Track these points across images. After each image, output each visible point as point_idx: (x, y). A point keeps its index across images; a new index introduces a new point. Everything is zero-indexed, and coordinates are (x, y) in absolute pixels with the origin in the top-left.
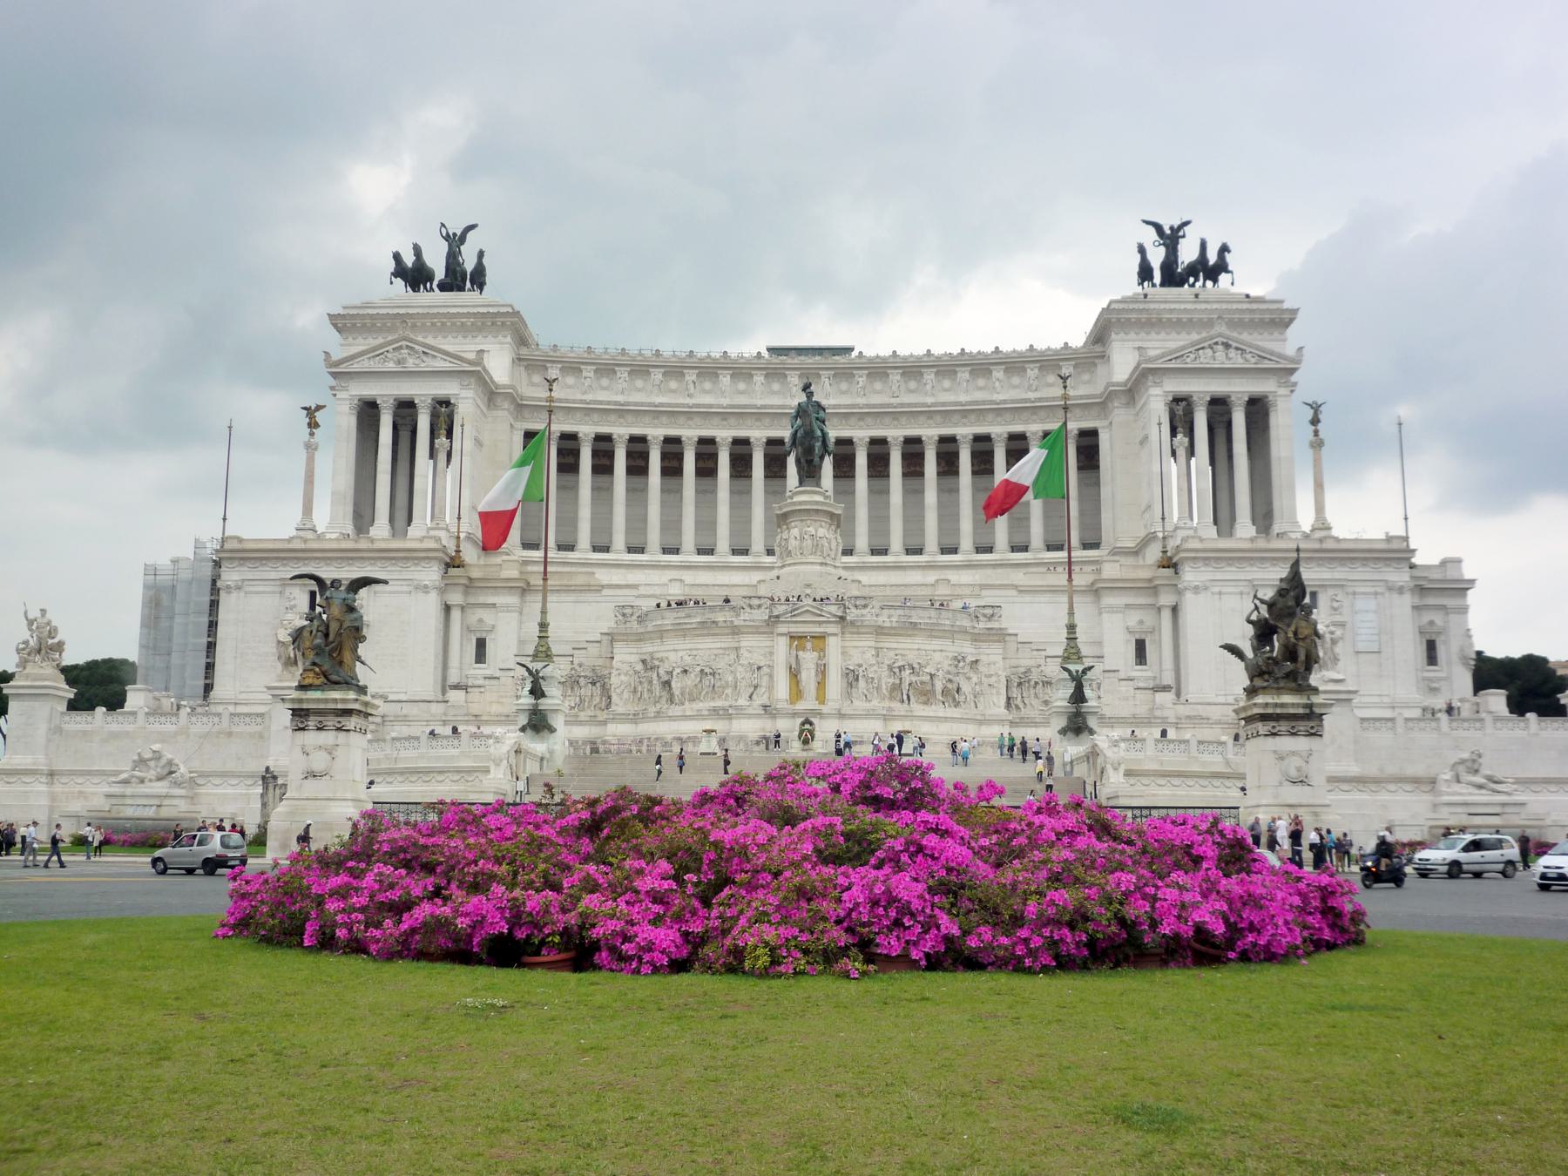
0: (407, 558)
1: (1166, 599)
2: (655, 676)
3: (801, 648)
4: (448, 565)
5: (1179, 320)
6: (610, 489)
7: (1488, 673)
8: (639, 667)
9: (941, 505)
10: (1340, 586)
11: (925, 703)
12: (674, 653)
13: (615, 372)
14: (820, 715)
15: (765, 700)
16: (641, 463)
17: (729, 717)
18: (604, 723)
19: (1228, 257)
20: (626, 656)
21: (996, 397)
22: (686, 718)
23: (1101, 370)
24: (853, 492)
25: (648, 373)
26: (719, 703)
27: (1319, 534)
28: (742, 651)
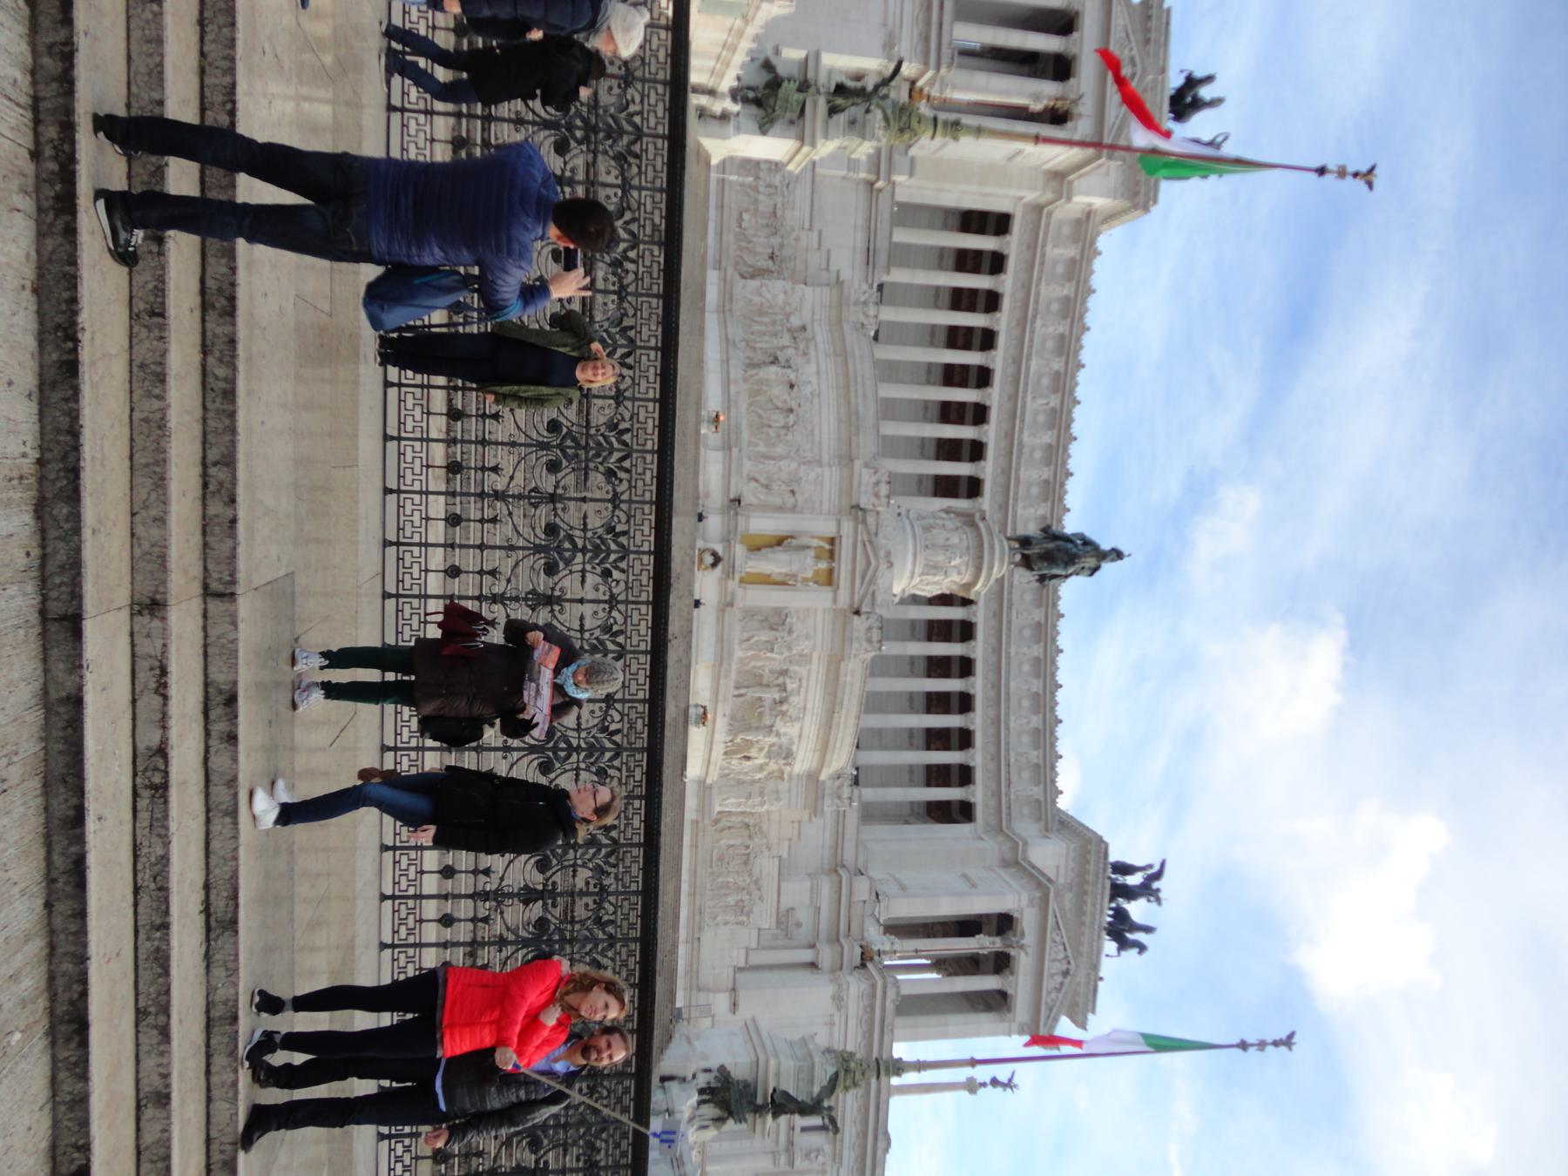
0: (928, 24)
1: (826, 955)
4: (913, 83)
5: (1084, 913)
8: (795, 321)
11: (733, 718)
12: (817, 373)
13: (1065, 317)
15: (748, 498)
16: (961, 341)
17: (727, 447)
18: (718, 265)
19: (1135, 951)
20: (810, 302)
22: (727, 384)
25: (1060, 354)
26: (745, 436)
28: (818, 470)
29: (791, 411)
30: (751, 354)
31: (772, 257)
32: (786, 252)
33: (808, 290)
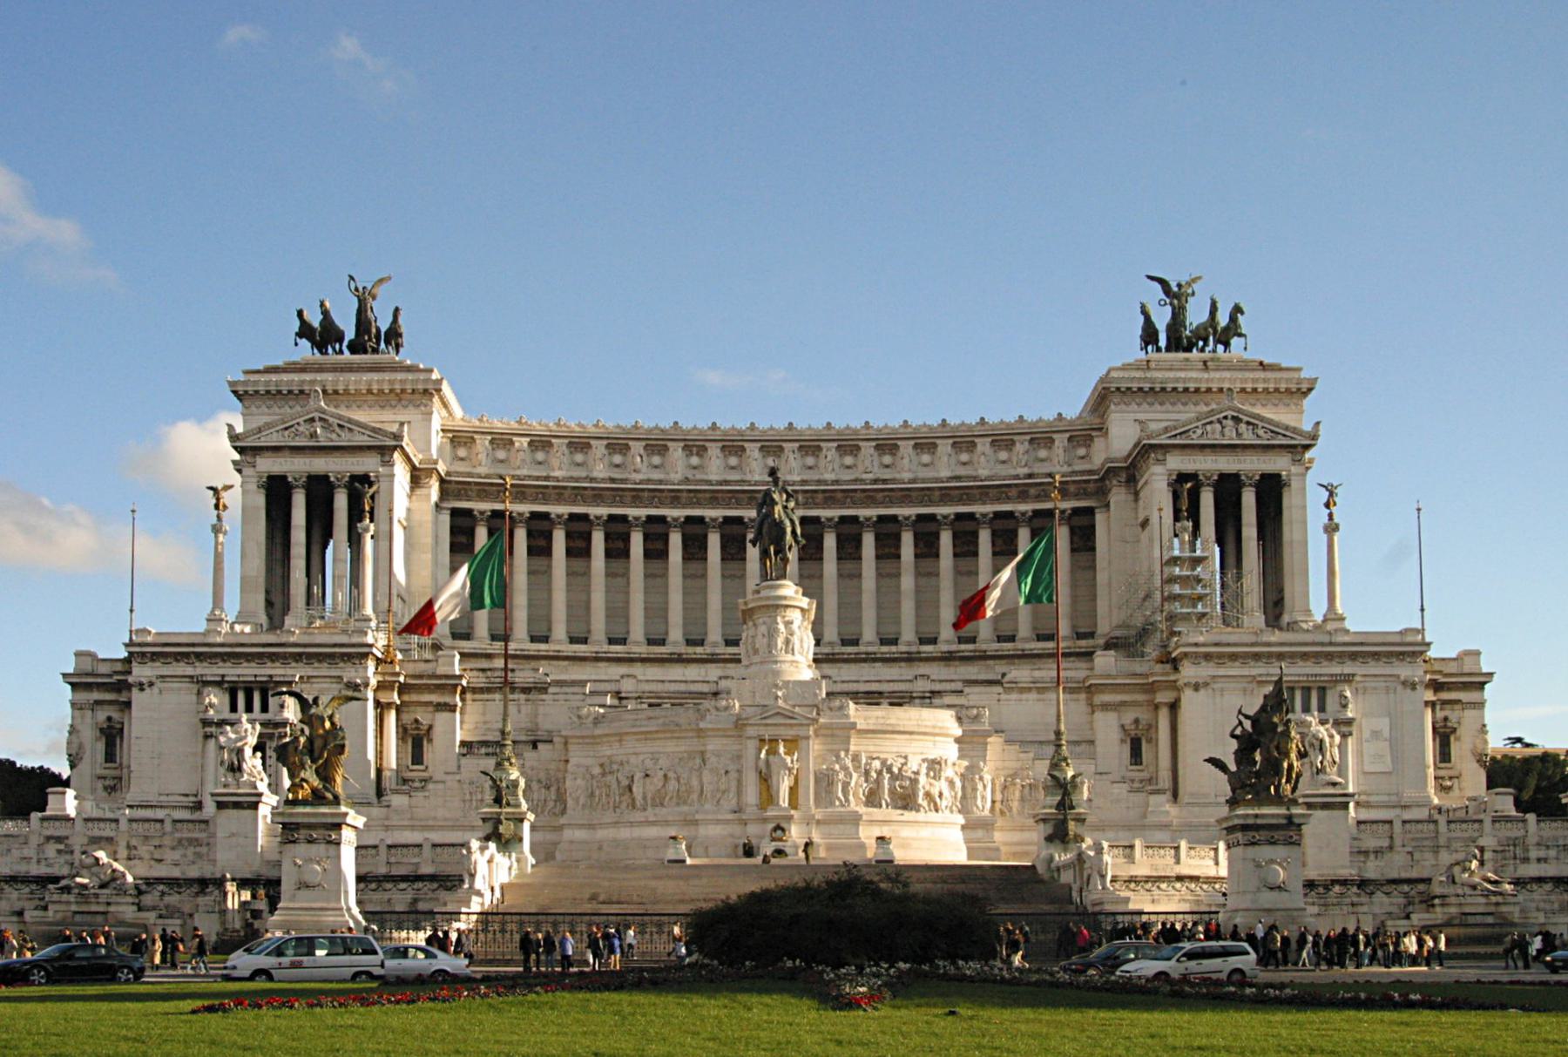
2: (614, 782)
3: (773, 752)
4: (378, 659)
6: (548, 571)
7: (1501, 772)
8: (597, 771)
9: (918, 590)
10: (1348, 679)
11: (905, 808)
12: (636, 754)
14: (790, 818)
17: (695, 823)
21: (983, 473)
23: (1098, 444)
24: (821, 576)
27: (1330, 626)
29: (665, 776)
30: (624, 805)
31: (548, 788)
32: (542, 776)
33: (573, 761)
